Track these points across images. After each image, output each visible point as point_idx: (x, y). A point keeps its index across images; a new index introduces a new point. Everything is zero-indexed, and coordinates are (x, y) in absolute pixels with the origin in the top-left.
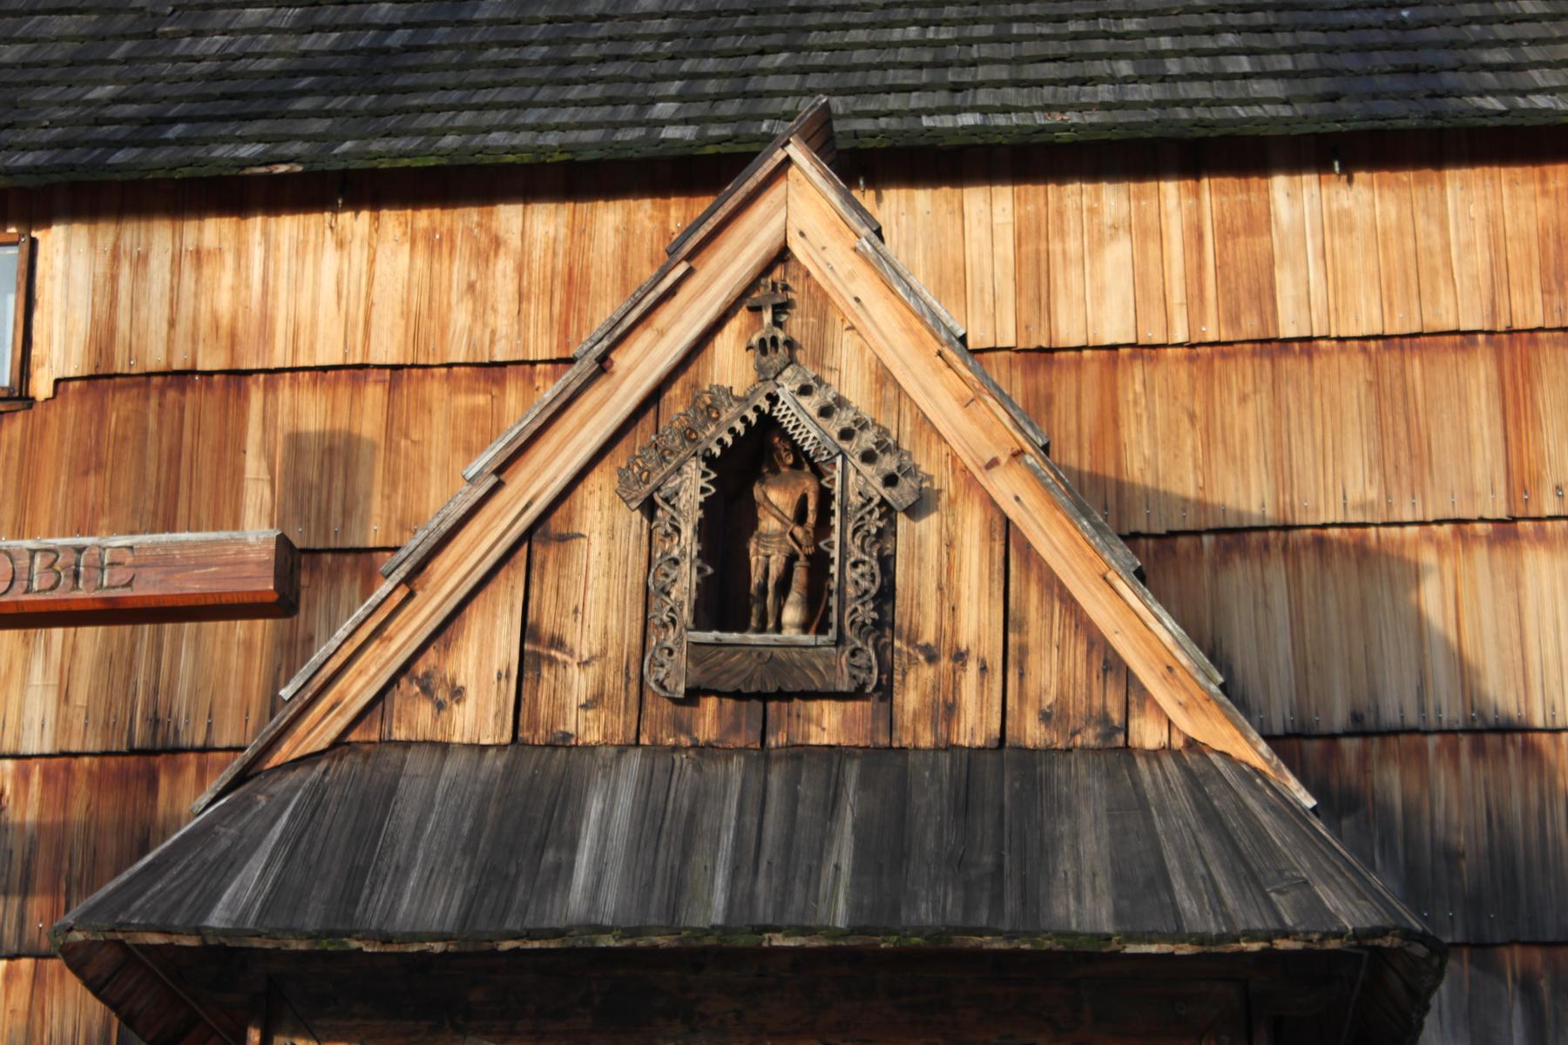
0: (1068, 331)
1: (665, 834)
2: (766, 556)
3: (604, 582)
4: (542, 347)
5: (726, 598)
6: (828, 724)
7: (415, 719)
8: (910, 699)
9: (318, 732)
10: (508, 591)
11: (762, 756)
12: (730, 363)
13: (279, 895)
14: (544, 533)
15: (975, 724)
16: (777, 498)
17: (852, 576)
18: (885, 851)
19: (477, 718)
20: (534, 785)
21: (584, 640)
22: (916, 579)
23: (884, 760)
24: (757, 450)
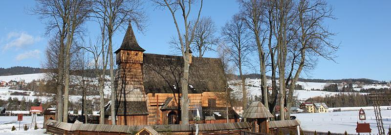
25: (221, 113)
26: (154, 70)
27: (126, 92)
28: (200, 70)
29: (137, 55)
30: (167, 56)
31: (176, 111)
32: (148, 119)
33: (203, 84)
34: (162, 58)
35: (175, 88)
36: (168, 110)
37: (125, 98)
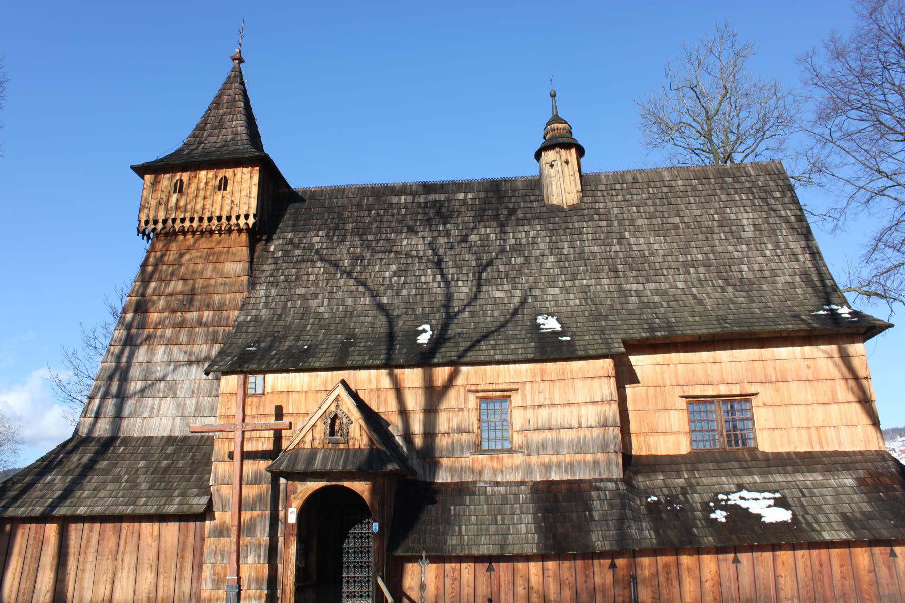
0: (382, 387)
1: (325, 459)
2: (337, 428)
3: (321, 431)
4: (323, 389)
5: (332, 433)
6: (342, 446)
7: (302, 446)
8: (351, 443)
9: (291, 447)
10: (310, 432)
11: (336, 449)
12: (333, 408)
13: (287, 466)
14: (314, 425)
15: (357, 447)
16: (338, 422)
17: (345, 431)
18: (346, 461)
19: (308, 445)
20: (313, 452)
21: (318, 437)
22: (352, 430)
23: (348, 450)
24: (335, 417)
25: (792, 495)
26: (322, 260)
27: (135, 386)
28: (638, 228)
29: (223, 185)
30: (429, 188)
31: (361, 487)
32: (210, 542)
33: (647, 305)
34: (395, 200)
35: (423, 339)
36: (304, 476)
37: (118, 416)
